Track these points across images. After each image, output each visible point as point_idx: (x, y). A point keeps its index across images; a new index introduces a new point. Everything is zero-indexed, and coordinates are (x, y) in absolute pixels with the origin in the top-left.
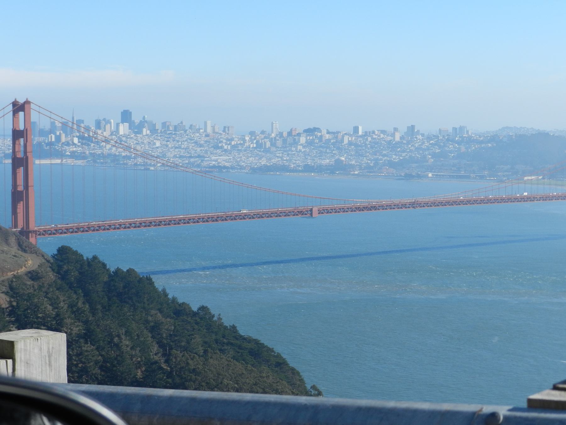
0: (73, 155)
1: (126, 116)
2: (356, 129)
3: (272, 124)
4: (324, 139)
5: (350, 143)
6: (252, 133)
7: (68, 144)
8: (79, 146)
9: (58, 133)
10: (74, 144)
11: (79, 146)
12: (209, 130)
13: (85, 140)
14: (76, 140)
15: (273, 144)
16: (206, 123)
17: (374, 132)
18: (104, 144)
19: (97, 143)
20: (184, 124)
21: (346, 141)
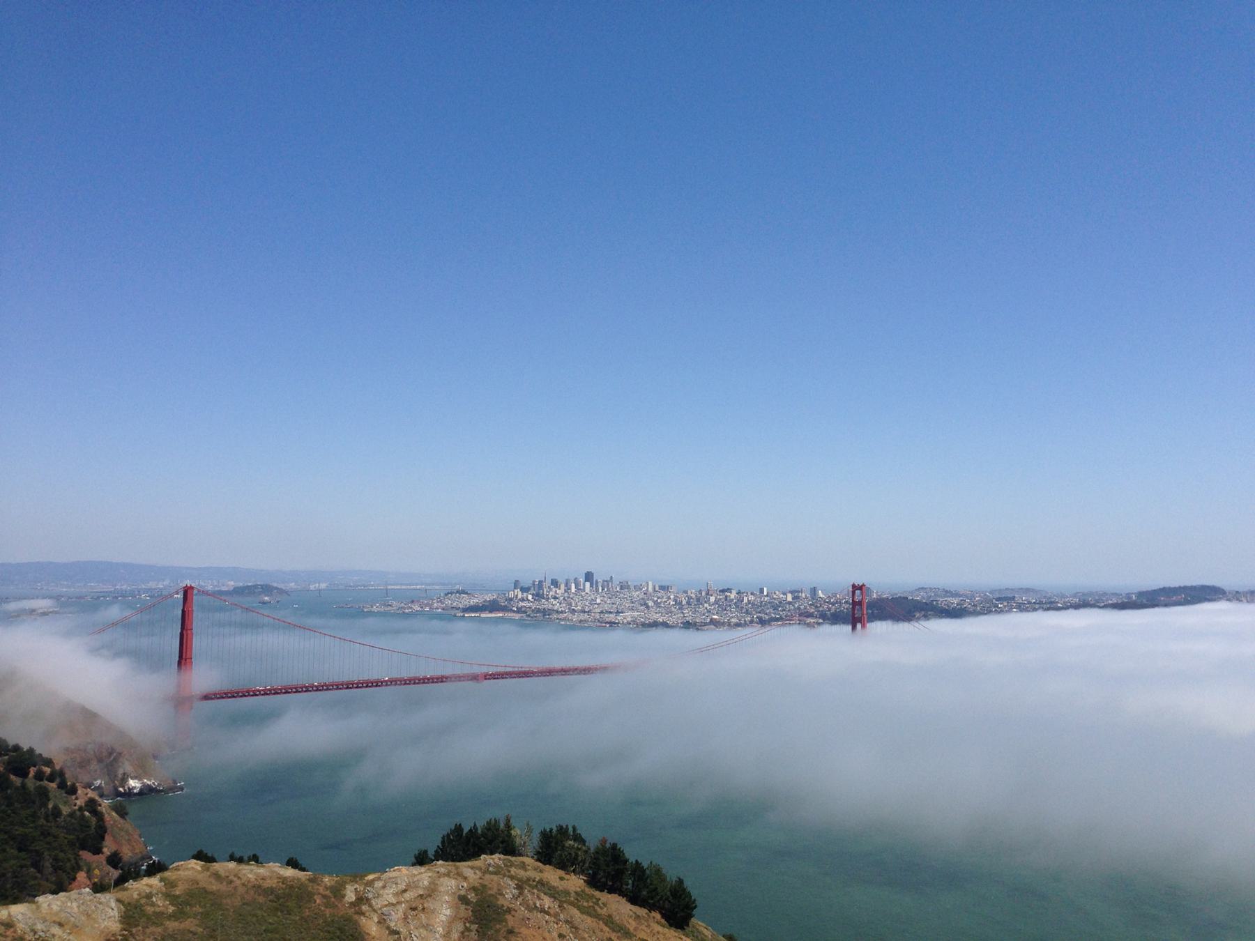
0: (519, 611)
1: (589, 577)
2: (762, 591)
3: (708, 584)
4: (728, 599)
5: (749, 602)
6: (686, 592)
7: (523, 600)
8: (531, 602)
9: (516, 594)
10: (528, 600)
11: (531, 602)
12: (650, 589)
13: (538, 596)
14: (530, 597)
15: (688, 603)
16: (647, 583)
17: (775, 593)
18: (552, 600)
19: (548, 599)
20: (629, 583)
21: (745, 600)
